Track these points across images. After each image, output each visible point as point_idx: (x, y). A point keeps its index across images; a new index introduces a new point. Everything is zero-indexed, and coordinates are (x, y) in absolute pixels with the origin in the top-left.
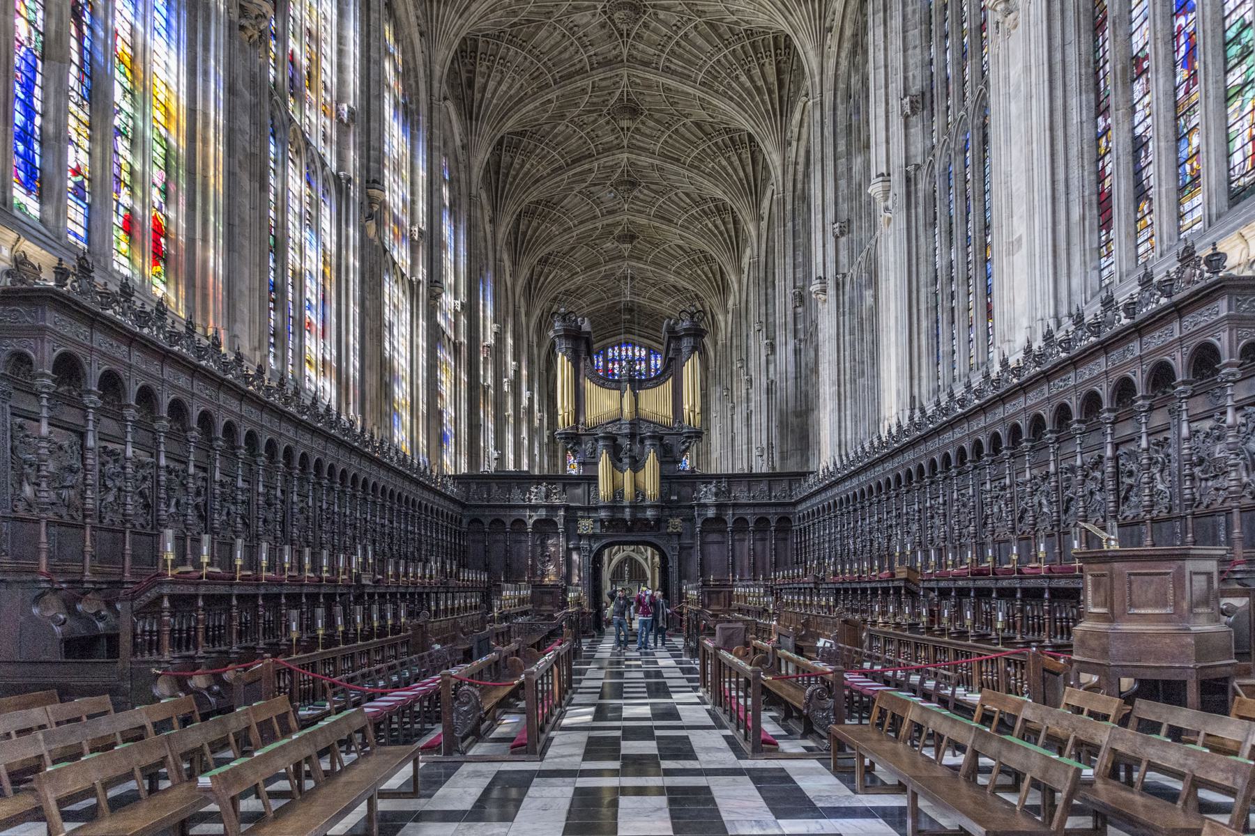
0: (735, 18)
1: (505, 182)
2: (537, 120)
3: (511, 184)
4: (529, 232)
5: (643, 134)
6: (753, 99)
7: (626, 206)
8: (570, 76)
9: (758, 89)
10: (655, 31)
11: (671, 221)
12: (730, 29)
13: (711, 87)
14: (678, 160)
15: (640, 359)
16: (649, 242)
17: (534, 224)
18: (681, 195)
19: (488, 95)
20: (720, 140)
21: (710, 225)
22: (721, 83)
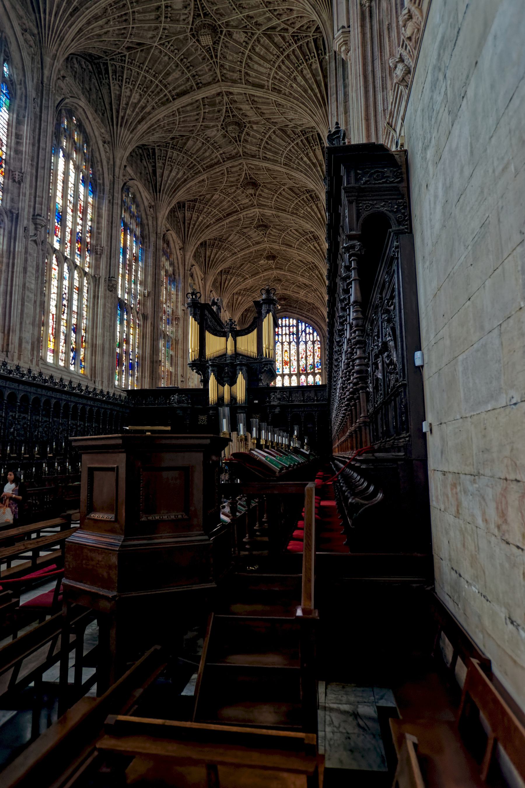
0: (292, 124)
1: (189, 228)
2: (200, 192)
3: (193, 228)
4: (212, 256)
5: (264, 197)
6: (312, 170)
7: (266, 239)
8: (211, 166)
9: (313, 164)
10: (254, 137)
11: (291, 246)
12: (293, 131)
13: (290, 166)
14: (285, 211)
15: (293, 326)
16: (284, 259)
17: (214, 251)
18: (293, 231)
19: (165, 178)
20: (304, 197)
21: (312, 247)
22: (294, 163)
